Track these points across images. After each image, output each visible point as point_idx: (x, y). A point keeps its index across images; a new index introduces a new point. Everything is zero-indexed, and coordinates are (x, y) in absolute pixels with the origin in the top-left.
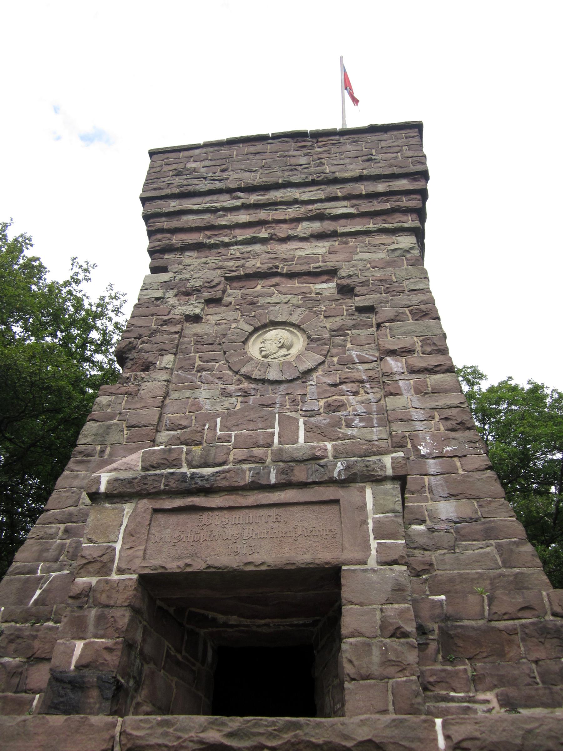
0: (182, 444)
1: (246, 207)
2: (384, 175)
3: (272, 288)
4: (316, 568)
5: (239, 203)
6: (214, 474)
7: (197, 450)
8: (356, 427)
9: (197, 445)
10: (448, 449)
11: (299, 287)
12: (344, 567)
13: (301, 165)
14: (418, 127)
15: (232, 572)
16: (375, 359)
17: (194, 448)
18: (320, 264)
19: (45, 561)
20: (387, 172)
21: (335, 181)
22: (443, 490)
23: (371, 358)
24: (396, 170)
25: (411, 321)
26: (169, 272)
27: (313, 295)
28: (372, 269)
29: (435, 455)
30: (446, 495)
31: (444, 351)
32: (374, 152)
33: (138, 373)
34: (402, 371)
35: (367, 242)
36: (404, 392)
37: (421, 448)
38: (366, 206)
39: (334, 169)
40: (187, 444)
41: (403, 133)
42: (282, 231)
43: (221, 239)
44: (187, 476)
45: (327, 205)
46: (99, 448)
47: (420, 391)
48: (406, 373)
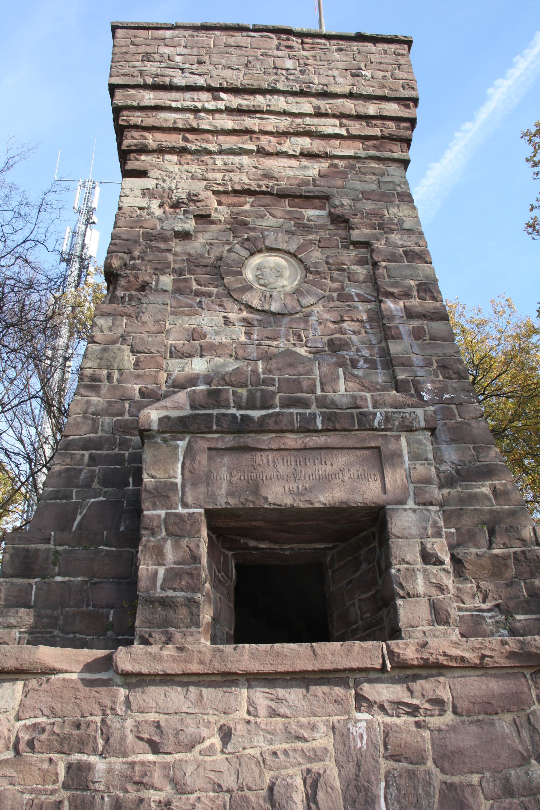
0: (228, 385)
1: (229, 111)
2: (375, 96)
3: (263, 209)
4: (364, 507)
5: (221, 105)
6: (264, 417)
7: (243, 392)
8: (361, 368)
9: (241, 387)
10: (447, 396)
11: (291, 211)
12: (388, 507)
13: (287, 70)
14: (409, 43)
15: (289, 508)
16: (374, 299)
17: (240, 390)
18: (311, 187)
19: (77, 487)
20: (379, 92)
21: (324, 95)
22: (445, 435)
23: (370, 297)
24: (386, 92)
25: (406, 263)
26: (149, 177)
27: (305, 221)
28: (365, 201)
29: (436, 402)
30: (448, 440)
31: (435, 295)
32: (362, 66)
33: (133, 293)
34: (401, 315)
35: (357, 169)
36: (405, 337)
37: (424, 394)
38: (357, 128)
39: (324, 81)
40: (232, 386)
41: (392, 47)
42: (266, 142)
43: (204, 145)
44: (237, 417)
45: (316, 121)
46: (105, 372)
47: (417, 334)
48: (405, 318)
